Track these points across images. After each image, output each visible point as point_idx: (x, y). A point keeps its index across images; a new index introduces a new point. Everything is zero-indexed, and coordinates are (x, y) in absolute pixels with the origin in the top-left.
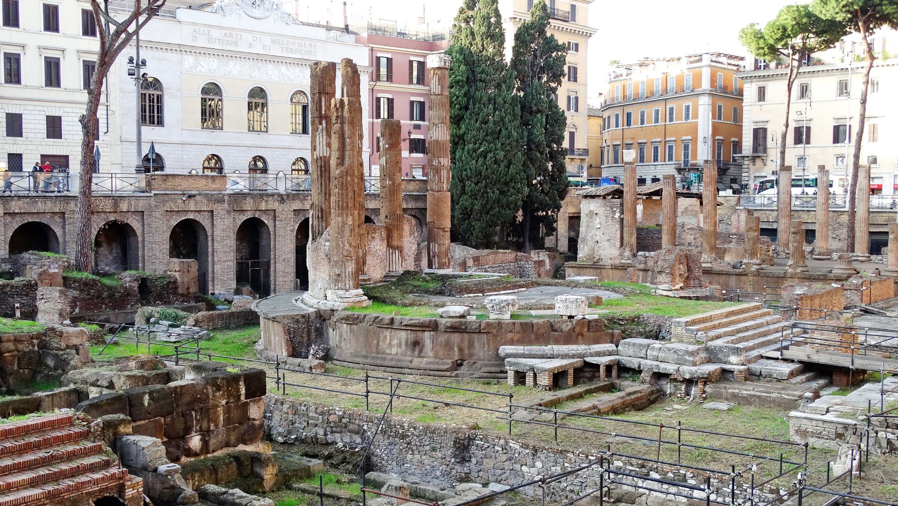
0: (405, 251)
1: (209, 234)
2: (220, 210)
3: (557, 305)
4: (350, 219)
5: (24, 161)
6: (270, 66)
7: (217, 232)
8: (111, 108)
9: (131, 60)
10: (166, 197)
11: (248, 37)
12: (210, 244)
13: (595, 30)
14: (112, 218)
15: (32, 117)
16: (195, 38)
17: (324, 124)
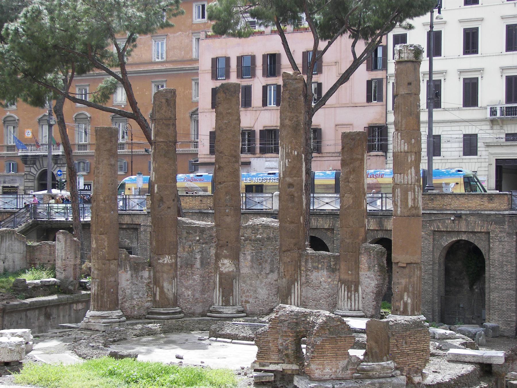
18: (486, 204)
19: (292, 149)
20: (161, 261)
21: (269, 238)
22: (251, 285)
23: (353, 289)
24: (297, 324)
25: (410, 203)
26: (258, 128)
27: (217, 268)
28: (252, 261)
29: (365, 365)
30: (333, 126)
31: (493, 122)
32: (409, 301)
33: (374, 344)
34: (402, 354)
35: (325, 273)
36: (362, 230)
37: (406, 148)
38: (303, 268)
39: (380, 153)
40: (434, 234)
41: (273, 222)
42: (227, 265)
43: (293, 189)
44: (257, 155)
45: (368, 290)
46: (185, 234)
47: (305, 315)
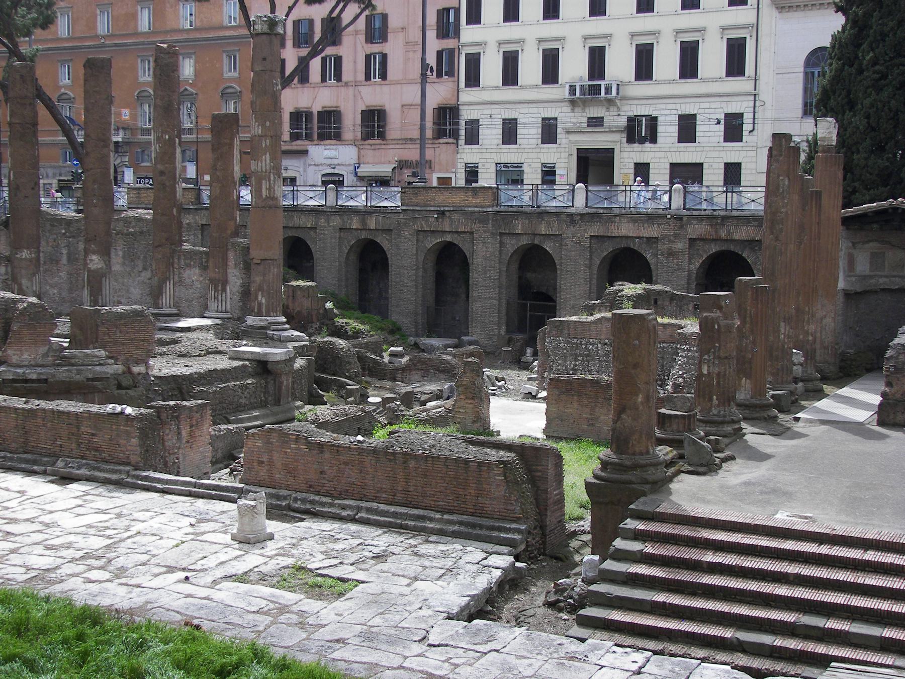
8: (762, 97)
18: (470, 199)
19: (162, 132)
20: (18, 256)
21: (142, 233)
22: (123, 284)
23: (220, 288)
24: (6, 310)
25: (264, 193)
26: (316, 108)
27: (86, 264)
28: (124, 257)
29: (67, 353)
30: (399, 106)
31: (573, 103)
32: (264, 301)
33: (78, 332)
34: (116, 343)
35: (197, 271)
36: (232, 223)
37: (260, 132)
38: (176, 266)
39: (451, 140)
40: (418, 235)
41: (148, 214)
42: (96, 262)
43: (164, 178)
44: (315, 142)
45: (235, 290)
46: (48, 226)
47: (15, 302)
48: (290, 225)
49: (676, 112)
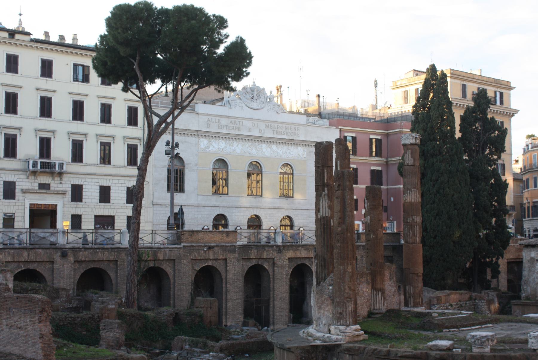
0: (387, 292)
1: (224, 277)
2: (232, 258)
3: (530, 341)
4: (350, 267)
5: (83, 220)
6: (264, 145)
7: (230, 276)
9: (168, 144)
10: (192, 248)
11: (248, 124)
12: (224, 285)
13: (517, 111)
14: (151, 265)
15: (117, 188)
16: (208, 125)
17: (326, 191)
18: (225, 238)
48: (96, 259)
49: (98, 184)
